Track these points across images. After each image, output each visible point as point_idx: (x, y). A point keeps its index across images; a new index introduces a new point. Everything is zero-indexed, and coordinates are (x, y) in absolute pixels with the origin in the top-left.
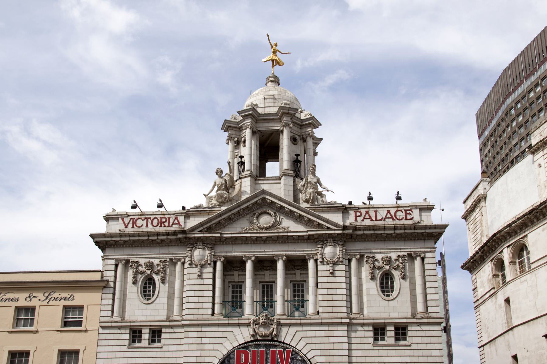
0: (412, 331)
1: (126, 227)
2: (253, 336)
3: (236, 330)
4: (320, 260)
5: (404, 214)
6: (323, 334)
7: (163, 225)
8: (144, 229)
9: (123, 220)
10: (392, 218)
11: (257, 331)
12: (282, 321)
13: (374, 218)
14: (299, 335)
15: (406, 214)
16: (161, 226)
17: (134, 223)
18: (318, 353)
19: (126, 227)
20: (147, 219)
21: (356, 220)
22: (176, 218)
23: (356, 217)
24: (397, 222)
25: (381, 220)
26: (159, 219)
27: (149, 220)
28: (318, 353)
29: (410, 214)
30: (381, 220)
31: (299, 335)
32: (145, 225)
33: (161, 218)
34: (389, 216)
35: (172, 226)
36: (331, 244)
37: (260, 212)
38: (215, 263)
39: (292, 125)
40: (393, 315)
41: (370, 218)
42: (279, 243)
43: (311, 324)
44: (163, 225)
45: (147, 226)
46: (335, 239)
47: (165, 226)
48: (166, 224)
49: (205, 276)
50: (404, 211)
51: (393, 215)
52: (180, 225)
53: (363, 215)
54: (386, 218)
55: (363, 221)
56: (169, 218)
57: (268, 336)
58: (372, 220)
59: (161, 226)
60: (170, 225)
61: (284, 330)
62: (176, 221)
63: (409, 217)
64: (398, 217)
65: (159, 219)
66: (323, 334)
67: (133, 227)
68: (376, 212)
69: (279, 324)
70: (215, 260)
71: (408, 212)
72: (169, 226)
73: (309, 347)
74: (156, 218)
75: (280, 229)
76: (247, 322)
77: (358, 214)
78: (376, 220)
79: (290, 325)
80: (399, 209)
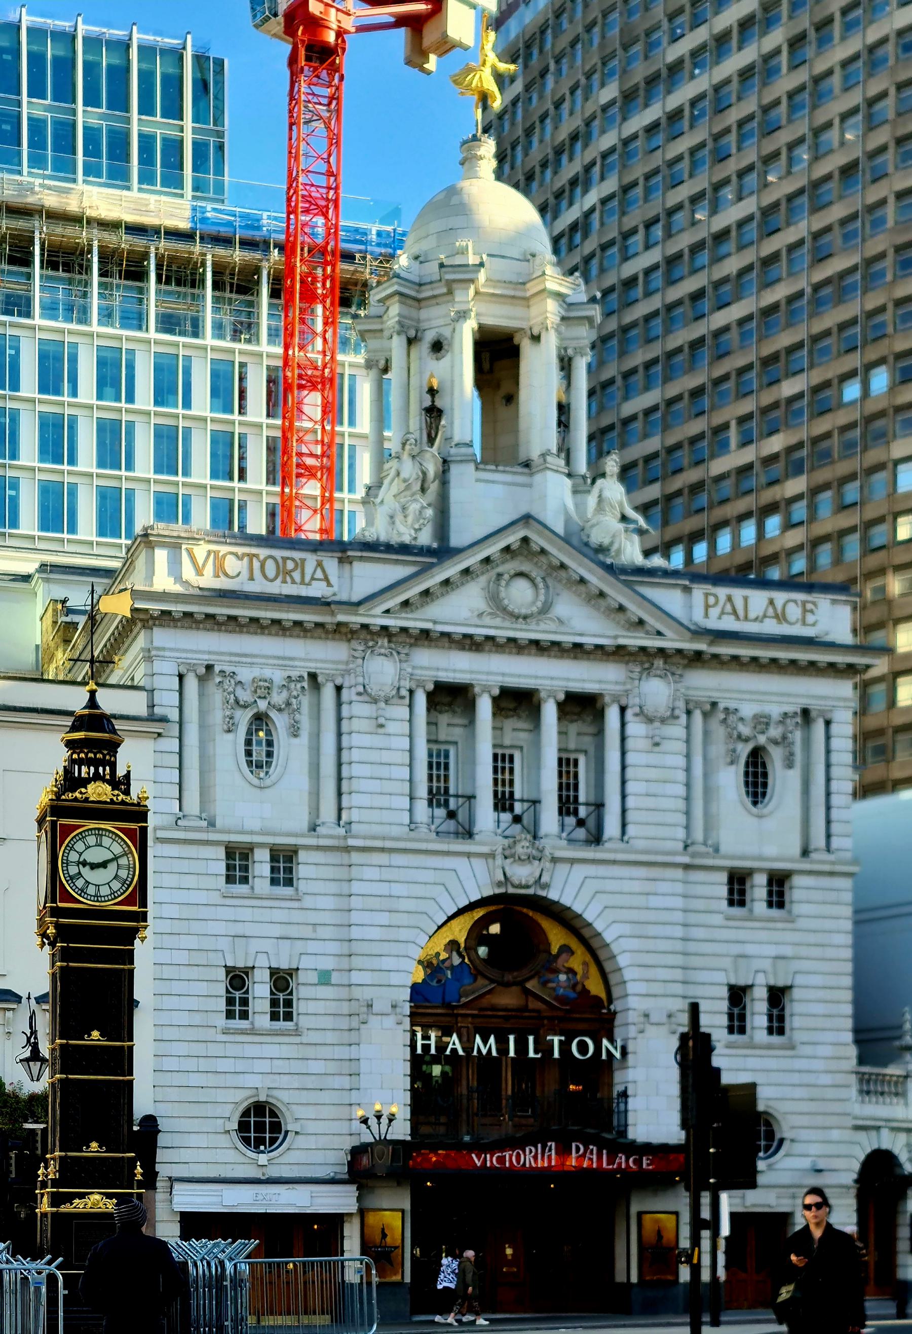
0: (800, 889)
2: (499, 884)
3: (461, 864)
4: (637, 710)
6: (636, 886)
7: (288, 579)
11: (508, 875)
12: (559, 854)
14: (592, 886)
16: (284, 582)
18: (626, 929)
22: (319, 564)
26: (280, 561)
27: (255, 560)
28: (626, 929)
31: (592, 886)
32: (245, 574)
33: (285, 559)
35: (309, 584)
36: (658, 672)
40: (770, 850)
43: (614, 862)
44: (288, 579)
45: (251, 578)
47: (293, 582)
48: (297, 575)
52: (329, 585)
59: (284, 582)
60: (307, 579)
61: (562, 869)
62: (319, 574)
65: (280, 561)
66: (636, 886)
69: (554, 860)
72: (303, 582)
73: (610, 915)
74: (271, 557)
79: (573, 861)
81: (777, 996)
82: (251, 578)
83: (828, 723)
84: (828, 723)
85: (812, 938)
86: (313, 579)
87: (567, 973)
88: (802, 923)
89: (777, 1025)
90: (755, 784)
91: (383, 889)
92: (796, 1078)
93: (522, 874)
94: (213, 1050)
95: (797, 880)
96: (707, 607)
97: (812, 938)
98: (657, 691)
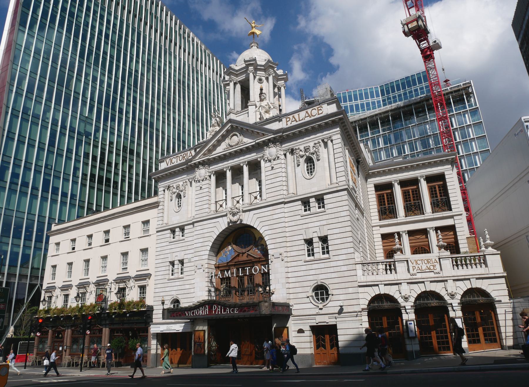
8: (176, 163)
12: (244, 209)
13: (298, 120)
17: (171, 161)
24: (313, 118)
29: (321, 110)
34: (307, 115)
38: (210, 176)
41: (296, 121)
46: (274, 141)
49: (203, 187)
51: (310, 113)
58: (297, 121)
64: (313, 115)
68: (299, 115)
70: (210, 174)
71: (319, 109)
73: (262, 224)
76: (225, 214)
77: (288, 119)
81: (324, 240)
83: (332, 141)
84: (332, 141)
85: (333, 216)
88: (328, 212)
89: (326, 250)
90: (311, 169)
91: (201, 232)
92: (332, 270)
93: (235, 219)
94: (166, 285)
95: (325, 197)
96: (287, 121)
97: (333, 216)
98: (272, 151)
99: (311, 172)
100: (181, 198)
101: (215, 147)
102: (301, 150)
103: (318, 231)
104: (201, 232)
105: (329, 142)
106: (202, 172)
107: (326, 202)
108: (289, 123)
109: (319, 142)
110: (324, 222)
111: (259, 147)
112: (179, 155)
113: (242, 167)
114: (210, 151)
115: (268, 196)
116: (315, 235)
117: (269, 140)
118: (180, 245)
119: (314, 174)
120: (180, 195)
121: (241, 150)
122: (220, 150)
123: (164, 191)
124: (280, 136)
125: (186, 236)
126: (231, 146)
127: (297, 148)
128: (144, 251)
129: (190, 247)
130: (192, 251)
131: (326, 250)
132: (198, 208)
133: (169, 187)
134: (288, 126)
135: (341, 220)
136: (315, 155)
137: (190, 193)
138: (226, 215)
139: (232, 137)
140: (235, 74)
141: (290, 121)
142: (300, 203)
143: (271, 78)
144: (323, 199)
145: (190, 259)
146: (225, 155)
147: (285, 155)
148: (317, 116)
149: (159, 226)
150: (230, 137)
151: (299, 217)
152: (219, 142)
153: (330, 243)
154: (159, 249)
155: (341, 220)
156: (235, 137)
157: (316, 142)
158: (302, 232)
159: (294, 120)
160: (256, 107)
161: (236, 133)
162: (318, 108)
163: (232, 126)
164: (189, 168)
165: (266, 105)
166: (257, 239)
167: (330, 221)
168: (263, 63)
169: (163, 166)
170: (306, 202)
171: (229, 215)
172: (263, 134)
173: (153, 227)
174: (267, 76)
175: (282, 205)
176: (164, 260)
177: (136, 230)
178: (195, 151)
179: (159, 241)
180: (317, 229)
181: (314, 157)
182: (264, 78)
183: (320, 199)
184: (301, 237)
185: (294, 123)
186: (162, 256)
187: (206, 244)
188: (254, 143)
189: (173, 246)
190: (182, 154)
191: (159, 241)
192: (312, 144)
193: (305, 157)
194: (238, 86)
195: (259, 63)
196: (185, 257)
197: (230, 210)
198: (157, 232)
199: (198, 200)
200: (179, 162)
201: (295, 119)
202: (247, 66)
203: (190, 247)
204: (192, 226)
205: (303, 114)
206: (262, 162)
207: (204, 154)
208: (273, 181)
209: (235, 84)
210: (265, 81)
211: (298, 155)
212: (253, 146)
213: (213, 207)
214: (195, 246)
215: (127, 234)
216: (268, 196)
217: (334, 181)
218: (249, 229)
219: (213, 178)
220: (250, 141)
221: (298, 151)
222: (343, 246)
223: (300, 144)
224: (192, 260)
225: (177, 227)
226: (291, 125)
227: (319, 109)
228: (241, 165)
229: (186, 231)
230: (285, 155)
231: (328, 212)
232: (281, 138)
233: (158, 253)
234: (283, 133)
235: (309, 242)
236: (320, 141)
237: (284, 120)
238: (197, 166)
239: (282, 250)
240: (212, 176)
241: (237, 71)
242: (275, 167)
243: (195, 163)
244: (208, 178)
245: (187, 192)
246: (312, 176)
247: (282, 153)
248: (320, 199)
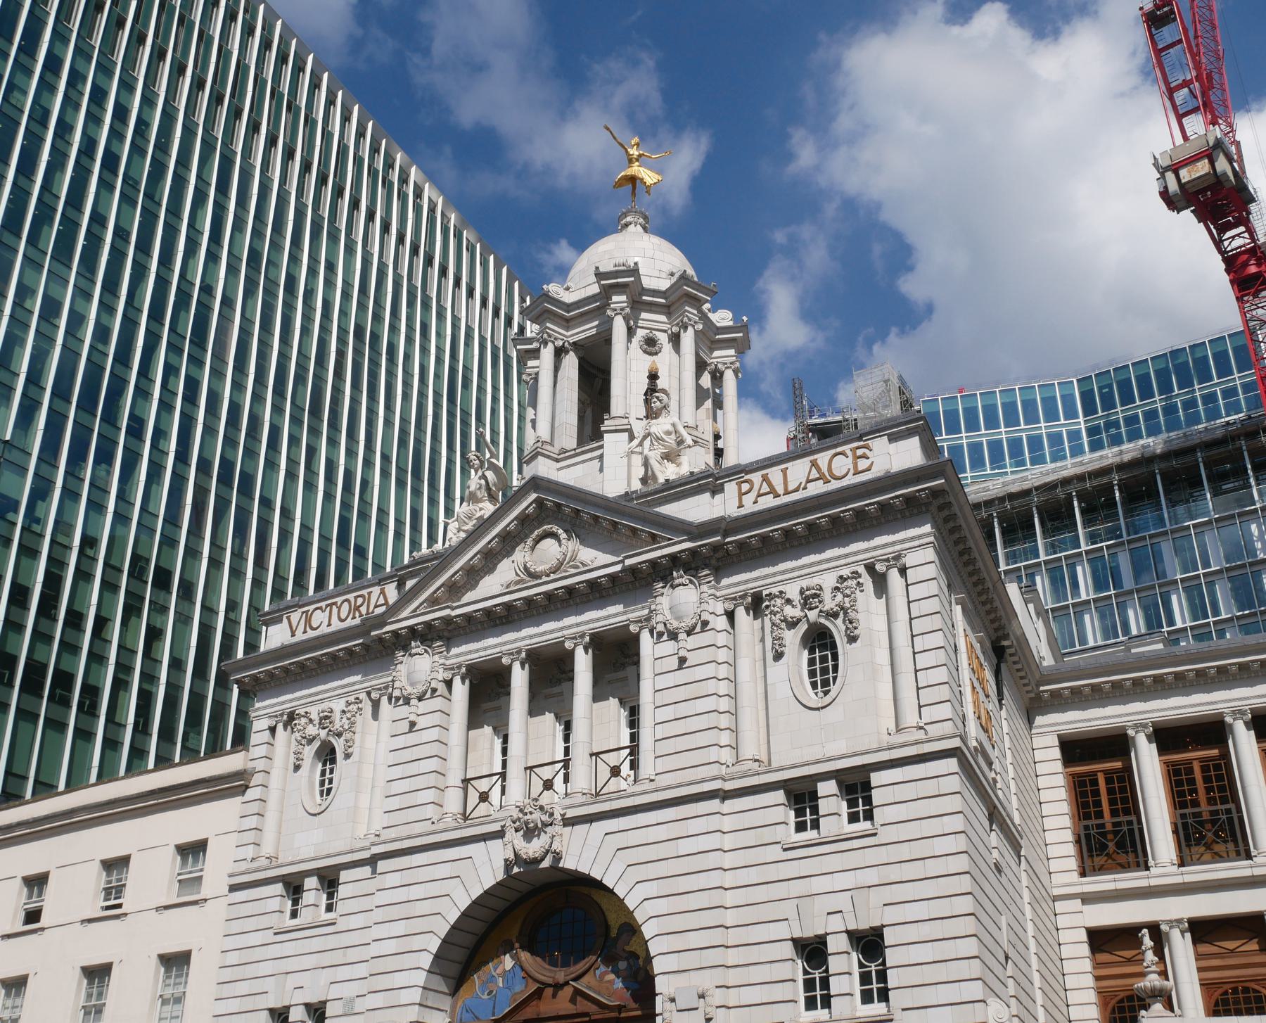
1: (293, 635)
5: (850, 459)
9: (288, 618)
10: (821, 477)
12: (571, 813)
13: (780, 490)
15: (857, 458)
16: (354, 618)
17: (308, 621)
19: (293, 635)
20: (331, 605)
21: (741, 506)
23: (741, 494)
24: (835, 485)
25: (796, 490)
29: (864, 456)
30: (796, 490)
33: (356, 598)
37: (534, 536)
38: (449, 684)
39: (628, 310)
42: (577, 604)
46: (691, 564)
49: (422, 722)
50: (849, 453)
51: (825, 469)
53: (756, 487)
54: (808, 481)
55: (755, 502)
56: (370, 593)
57: (542, 859)
63: (863, 464)
64: (837, 473)
67: (305, 632)
68: (784, 471)
70: (448, 675)
71: (859, 452)
75: (577, 567)
78: (787, 493)
80: (839, 449)
81: (870, 943)
82: (329, 625)
84: (903, 571)
85: (905, 852)
86: (376, 606)
87: (627, 959)
88: (885, 835)
89: (876, 987)
90: (825, 671)
91: (402, 895)
95: (876, 778)
97: (905, 852)
98: (682, 599)
99: (825, 683)
100: (333, 761)
101: (473, 575)
102: (789, 601)
103: (847, 907)
104: (402, 895)
105: (894, 575)
106: (420, 666)
107: (877, 797)
108: (748, 499)
109: (856, 575)
110: (871, 877)
111: (634, 584)
112: (339, 600)
113: (571, 654)
114: (453, 591)
115: (662, 765)
116: (836, 924)
117: (674, 558)
118: (316, 944)
119: (834, 689)
120: (333, 751)
121: (570, 590)
122: (495, 587)
123: (273, 730)
124: (716, 548)
125: (341, 907)
126: (534, 576)
127: (775, 591)
128: (176, 962)
129: (353, 955)
130: (361, 970)
131: (876, 987)
132: (395, 803)
133: (292, 717)
134: (743, 512)
135: (933, 867)
136: (839, 621)
137: (370, 742)
138: (500, 834)
139: (537, 541)
140: (562, 317)
141: (753, 495)
142: (779, 796)
143: (688, 339)
144: (867, 787)
145: (350, 1002)
146: (508, 606)
147: (730, 615)
148: (851, 480)
149: (243, 866)
150: (530, 541)
151: (775, 853)
152: (490, 559)
153: (892, 957)
154: (233, 958)
155: (933, 867)
156: (549, 542)
157: (846, 572)
158: (788, 909)
159: (765, 488)
160: (632, 438)
161: (555, 529)
162: (854, 450)
163: (539, 503)
164: (373, 649)
165: (668, 433)
166: (614, 933)
167: (894, 873)
168: (664, 285)
169: (275, 637)
170: (802, 796)
171: (510, 834)
172: (654, 538)
173: (216, 870)
174: (675, 329)
175: (714, 805)
176: (249, 1004)
177: (152, 877)
178: (401, 585)
179: (236, 926)
180: (842, 902)
181: (837, 629)
182: (663, 338)
183: (856, 786)
184: (782, 931)
185: (768, 502)
186: (243, 988)
187: (417, 942)
188: (618, 568)
189: (289, 949)
190: (351, 596)
191: (236, 926)
192: (828, 581)
193: (803, 627)
194: (571, 363)
195: (647, 283)
196: (334, 992)
197: (516, 814)
198: (234, 888)
199: (397, 772)
200: (337, 625)
201: (770, 485)
202: (606, 293)
203: (353, 955)
204: (367, 870)
205: (799, 470)
206: (646, 640)
207: (433, 602)
208: (683, 709)
209: (559, 353)
210: (667, 347)
211: (776, 619)
212: (612, 577)
213: (453, 801)
214: (375, 949)
215: (114, 891)
216: (662, 765)
217: (910, 718)
218: (585, 890)
219: (461, 690)
220: (603, 558)
221: (779, 601)
222: (941, 972)
223: (788, 578)
224: (360, 1005)
225: (308, 873)
226: (757, 508)
227: (859, 452)
228: (568, 645)
229: (343, 891)
230: (730, 615)
231: (885, 835)
232: (718, 553)
233: (228, 974)
234: (725, 535)
235: (813, 951)
236: (861, 570)
237: (731, 488)
238: (401, 642)
239: (706, 980)
240: (457, 681)
241: (569, 307)
242: (692, 658)
243: (395, 633)
244: (442, 688)
245: (357, 737)
246: (828, 699)
247: (720, 607)
248: (856, 786)
